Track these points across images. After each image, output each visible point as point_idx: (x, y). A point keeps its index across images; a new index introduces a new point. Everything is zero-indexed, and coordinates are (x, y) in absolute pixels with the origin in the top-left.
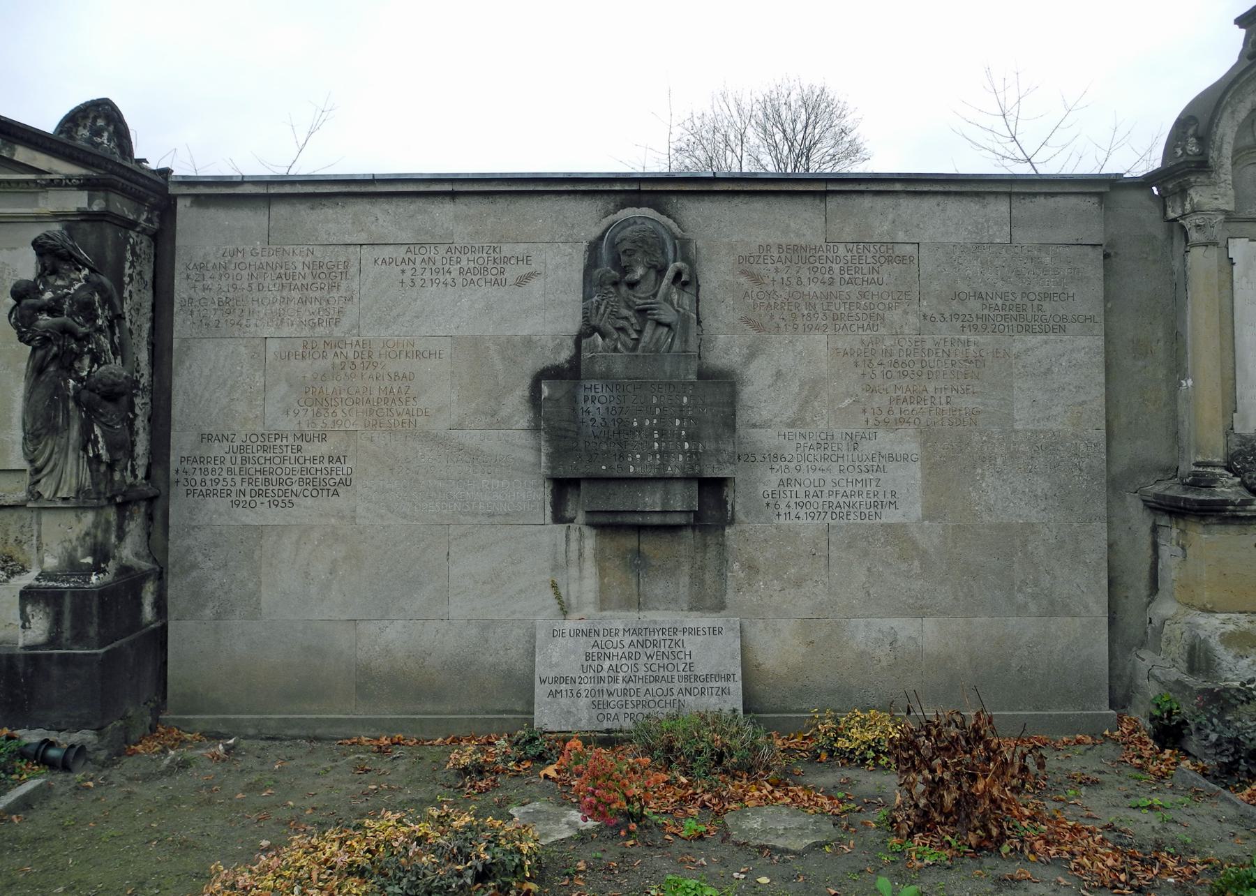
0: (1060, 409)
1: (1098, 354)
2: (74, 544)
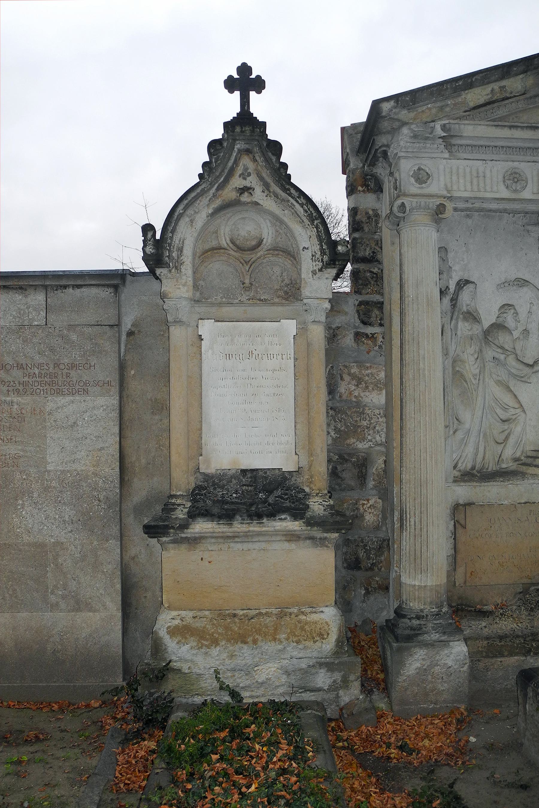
0: (83, 453)
1: (113, 410)
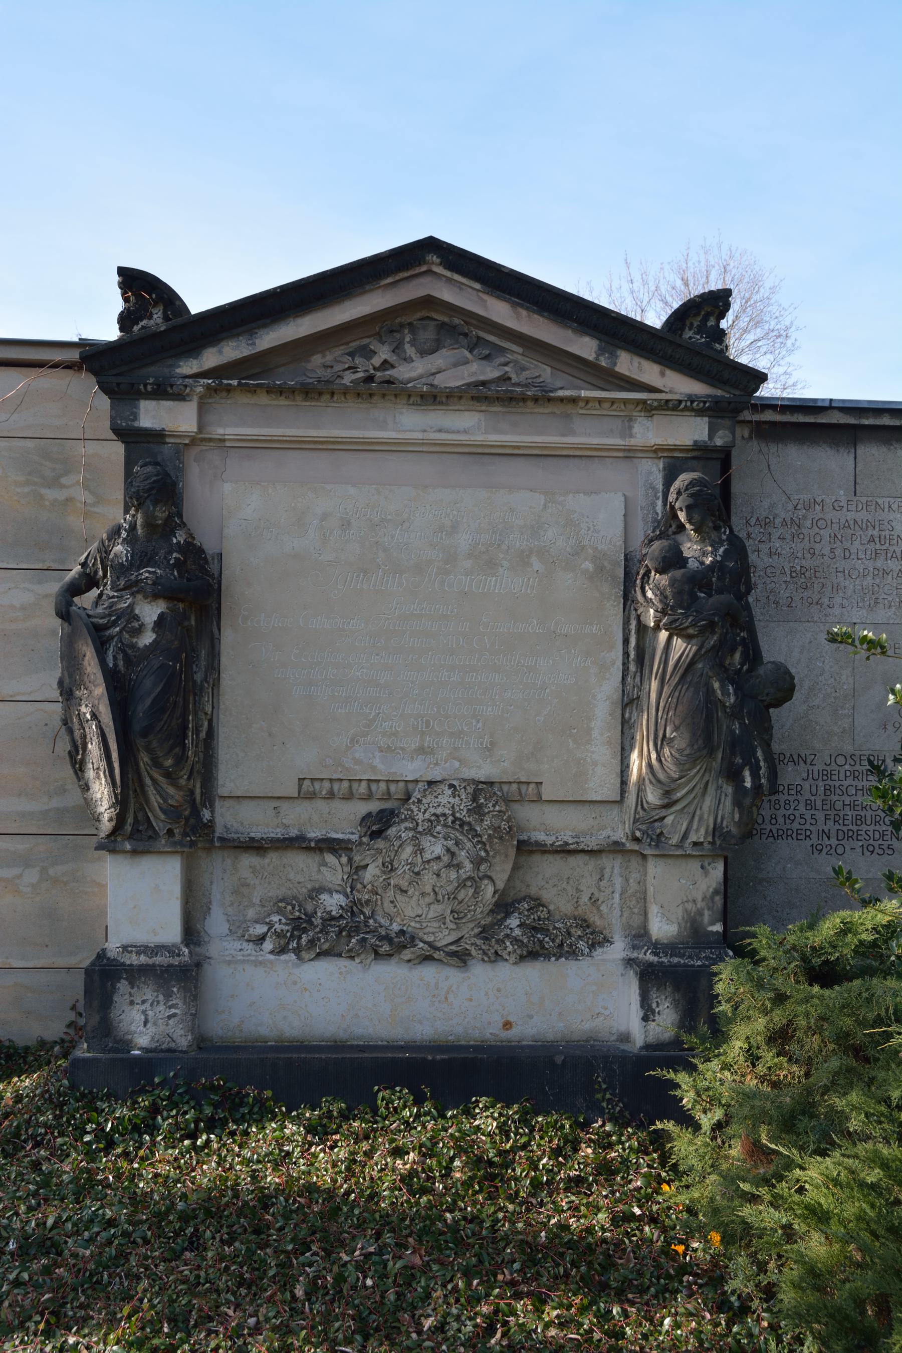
2: (699, 906)
